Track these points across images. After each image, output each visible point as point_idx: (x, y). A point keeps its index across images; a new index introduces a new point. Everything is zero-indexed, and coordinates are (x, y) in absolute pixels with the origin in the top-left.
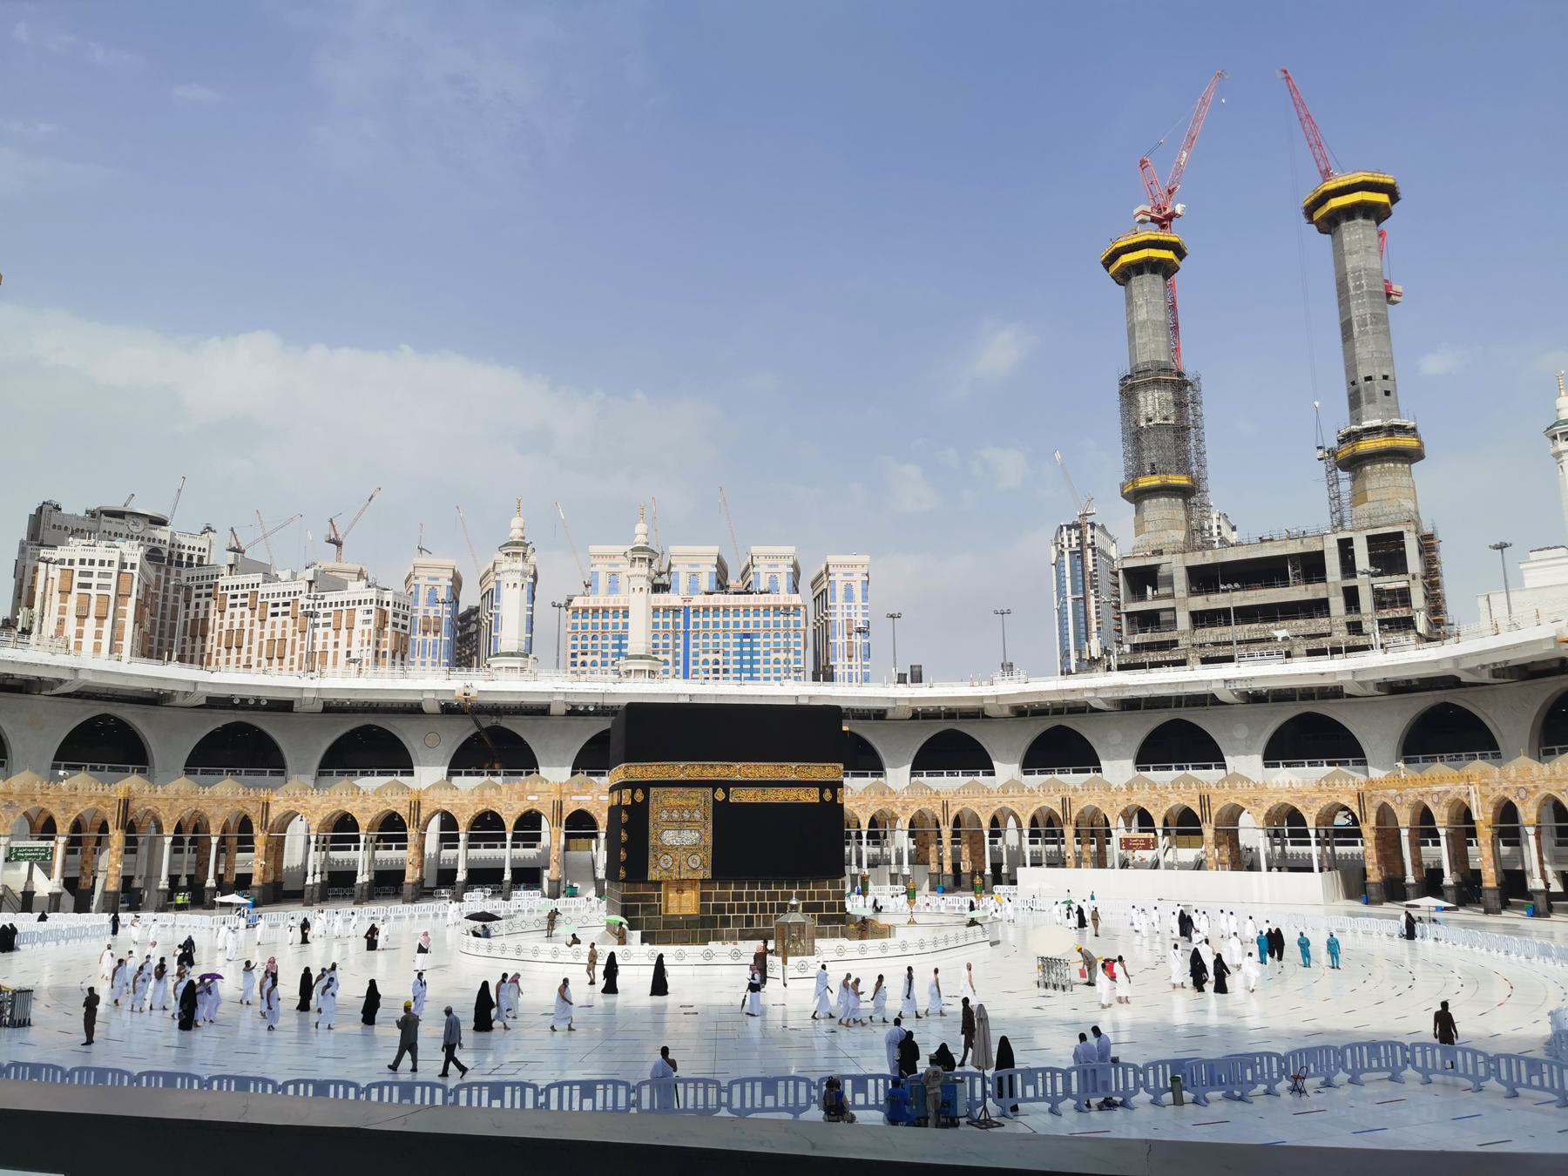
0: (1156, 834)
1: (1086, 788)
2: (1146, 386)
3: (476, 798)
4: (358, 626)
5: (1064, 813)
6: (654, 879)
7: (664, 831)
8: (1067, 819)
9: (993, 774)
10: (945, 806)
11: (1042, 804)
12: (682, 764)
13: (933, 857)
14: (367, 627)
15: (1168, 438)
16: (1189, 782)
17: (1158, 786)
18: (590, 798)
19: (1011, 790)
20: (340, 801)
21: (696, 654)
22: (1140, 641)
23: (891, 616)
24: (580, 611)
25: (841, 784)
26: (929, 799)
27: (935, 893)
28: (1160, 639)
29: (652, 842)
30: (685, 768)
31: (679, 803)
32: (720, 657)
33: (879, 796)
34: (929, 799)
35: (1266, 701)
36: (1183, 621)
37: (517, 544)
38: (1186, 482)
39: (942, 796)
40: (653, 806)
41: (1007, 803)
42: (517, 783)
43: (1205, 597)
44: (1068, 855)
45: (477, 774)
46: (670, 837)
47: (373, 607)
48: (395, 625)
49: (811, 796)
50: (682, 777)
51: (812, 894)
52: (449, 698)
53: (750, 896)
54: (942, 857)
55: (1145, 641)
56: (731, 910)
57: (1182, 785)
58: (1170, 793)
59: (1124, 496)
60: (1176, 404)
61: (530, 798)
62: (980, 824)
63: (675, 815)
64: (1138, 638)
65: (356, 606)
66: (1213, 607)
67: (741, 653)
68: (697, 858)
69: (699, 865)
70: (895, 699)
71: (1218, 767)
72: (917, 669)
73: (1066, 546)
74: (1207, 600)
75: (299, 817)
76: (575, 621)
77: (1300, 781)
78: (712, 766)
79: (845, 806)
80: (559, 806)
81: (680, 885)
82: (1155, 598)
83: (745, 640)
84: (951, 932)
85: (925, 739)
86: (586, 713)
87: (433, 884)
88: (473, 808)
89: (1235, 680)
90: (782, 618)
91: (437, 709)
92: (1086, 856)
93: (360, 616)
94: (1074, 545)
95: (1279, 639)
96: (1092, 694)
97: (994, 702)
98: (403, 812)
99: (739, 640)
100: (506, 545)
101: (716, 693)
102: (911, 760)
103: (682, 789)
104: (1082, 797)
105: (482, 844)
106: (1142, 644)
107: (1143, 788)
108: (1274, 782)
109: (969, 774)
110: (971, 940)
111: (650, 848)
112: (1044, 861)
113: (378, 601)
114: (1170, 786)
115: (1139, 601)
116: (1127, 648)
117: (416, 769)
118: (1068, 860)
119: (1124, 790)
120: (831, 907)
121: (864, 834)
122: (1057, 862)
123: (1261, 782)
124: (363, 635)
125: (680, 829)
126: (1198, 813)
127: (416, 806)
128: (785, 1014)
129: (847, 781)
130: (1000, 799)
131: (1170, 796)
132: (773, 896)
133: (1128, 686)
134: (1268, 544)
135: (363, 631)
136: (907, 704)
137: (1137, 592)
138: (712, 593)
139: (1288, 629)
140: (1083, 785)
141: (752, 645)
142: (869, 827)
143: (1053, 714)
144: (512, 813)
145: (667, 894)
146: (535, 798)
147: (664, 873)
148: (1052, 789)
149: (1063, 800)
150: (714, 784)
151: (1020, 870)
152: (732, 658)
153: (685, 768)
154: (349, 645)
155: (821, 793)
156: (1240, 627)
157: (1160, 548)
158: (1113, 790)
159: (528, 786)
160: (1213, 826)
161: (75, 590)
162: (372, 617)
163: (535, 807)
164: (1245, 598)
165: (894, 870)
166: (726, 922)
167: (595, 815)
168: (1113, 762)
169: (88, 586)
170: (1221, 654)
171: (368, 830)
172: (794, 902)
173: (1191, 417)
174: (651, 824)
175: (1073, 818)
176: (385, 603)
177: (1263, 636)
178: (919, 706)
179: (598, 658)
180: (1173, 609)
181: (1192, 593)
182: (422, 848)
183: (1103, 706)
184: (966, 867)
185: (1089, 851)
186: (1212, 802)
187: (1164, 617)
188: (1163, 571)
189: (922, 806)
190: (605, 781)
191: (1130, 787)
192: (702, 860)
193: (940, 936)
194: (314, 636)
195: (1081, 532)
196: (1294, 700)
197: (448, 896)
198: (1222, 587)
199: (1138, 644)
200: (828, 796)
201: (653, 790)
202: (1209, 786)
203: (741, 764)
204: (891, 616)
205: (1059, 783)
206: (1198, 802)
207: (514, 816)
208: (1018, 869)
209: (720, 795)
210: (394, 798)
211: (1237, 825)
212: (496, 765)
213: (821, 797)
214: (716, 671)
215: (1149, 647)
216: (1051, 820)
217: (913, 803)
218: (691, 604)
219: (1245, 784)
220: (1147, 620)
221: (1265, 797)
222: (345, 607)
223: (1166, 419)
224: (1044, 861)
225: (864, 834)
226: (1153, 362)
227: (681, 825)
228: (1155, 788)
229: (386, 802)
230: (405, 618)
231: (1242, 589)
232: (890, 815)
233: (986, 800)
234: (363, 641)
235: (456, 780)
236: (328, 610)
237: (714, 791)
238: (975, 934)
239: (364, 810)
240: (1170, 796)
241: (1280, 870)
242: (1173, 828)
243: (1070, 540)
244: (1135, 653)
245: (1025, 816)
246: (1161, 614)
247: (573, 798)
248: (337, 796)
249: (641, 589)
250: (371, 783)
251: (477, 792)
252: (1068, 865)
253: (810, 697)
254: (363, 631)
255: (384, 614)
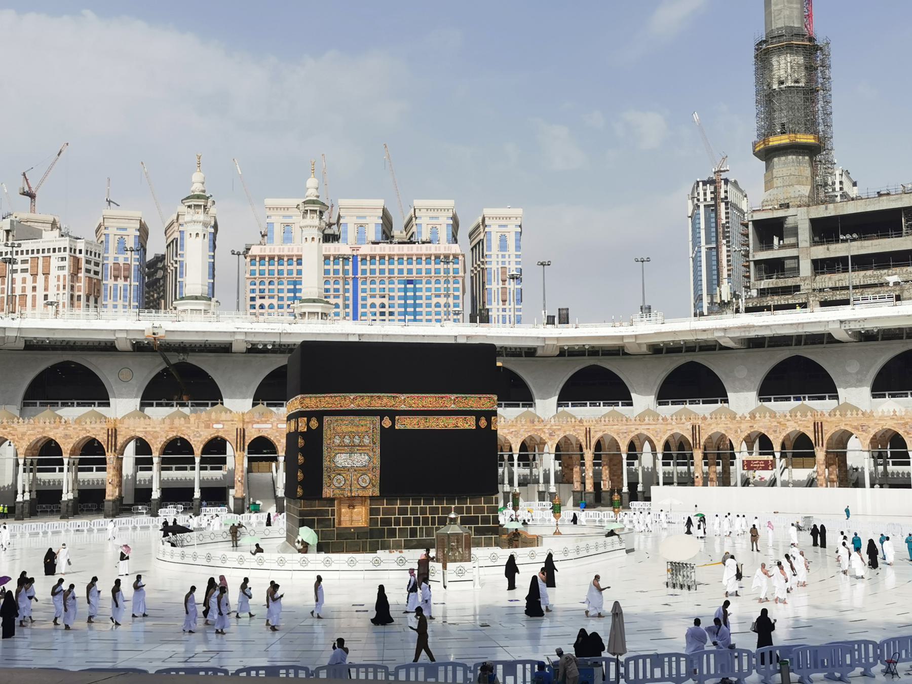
0: (774, 457)
1: (714, 416)
2: (780, 50)
3: (166, 426)
4: (54, 272)
5: (693, 435)
6: (328, 496)
7: (337, 454)
8: (696, 444)
9: (631, 404)
10: (588, 432)
11: (675, 431)
12: (352, 396)
13: (576, 477)
14: (61, 273)
15: (798, 100)
16: (805, 411)
17: (778, 415)
18: (270, 426)
19: (647, 419)
20: (44, 428)
21: (364, 299)
22: (766, 286)
23: (542, 264)
24: (258, 259)
25: (494, 413)
26: (574, 427)
27: (578, 508)
28: (784, 285)
29: (326, 464)
30: (355, 399)
31: (350, 429)
32: (386, 301)
33: (528, 424)
34: (574, 427)
35: (877, 340)
36: (806, 268)
37: (198, 197)
38: (813, 141)
39: (585, 424)
40: (327, 433)
41: (643, 430)
42: (204, 413)
43: (826, 246)
44: (696, 475)
45: (167, 405)
46: (342, 460)
47: (66, 254)
48: (88, 271)
49: (468, 423)
50: (353, 407)
51: (469, 509)
52: (139, 337)
53: (414, 511)
54: (584, 477)
55: (771, 286)
56: (397, 522)
57: (799, 414)
58: (788, 420)
59: (756, 154)
60: (806, 68)
61: (215, 426)
62: (618, 449)
63: (347, 441)
64: (765, 284)
65: (51, 254)
66: (833, 255)
67: (405, 298)
68: (367, 478)
69: (369, 484)
70: (545, 339)
71: (831, 398)
72: (565, 312)
73: (702, 200)
74: (828, 249)
75: (7, 443)
76: (253, 268)
77: (903, 410)
78: (379, 397)
79: (500, 433)
80: (242, 434)
81: (352, 502)
82: (781, 247)
83: (409, 286)
84: (591, 542)
85: (570, 374)
86: (265, 351)
87: (132, 502)
88: (165, 435)
89: (850, 321)
90: (442, 266)
91: (129, 348)
92: (712, 476)
93: (54, 263)
94: (709, 199)
95: (891, 284)
96: (721, 334)
97: (634, 340)
98: (102, 438)
99: (403, 286)
100: (188, 198)
101: (383, 333)
102: (558, 393)
103: (352, 417)
104: (710, 425)
105: (174, 466)
106: (768, 289)
107: (765, 417)
108: (880, 410)
109: (610, 405)
110: (609, 548)
111: (325, 469)
112: (675, 480)
113: (71, 249)
114: (788, 415)
115: (766, 250)
116: (754, 293)
117: (112, 401)
118: (696, 480)
119: (748, 418)
120: (486, 520)
121: (516, 457)
122: (687, 481)
123: (868, 411)
124: (58, 280)
125: (351, 453)
126: (812, 438)
127: (113, 433)
128: (445, 612)
129: (500, 411)
130: (637, 427)
131: (788, 423)
132: (434, 511)
133: (754, 326)
134: (884, 198)
135: (59, 277)
136: (555, 343)
137: (765, 241)
138: (378, 243)
139: (899, 275)
140: (711, 414)
141: (415, 290)
142: (520, 451)
143: (686, 351)
144: (199, 439)
145: (340, 510)
146: (220, 426)
147: (337, 491)
148: (683, 417)
149: (694, 428)
150: (381, 414)
151: (654, 489)
152: (397, 302)
153: (355, 399)
154: (46, 289)
155: (477, 421)
156: (856, 273)
157: (787, 201)
158: (738, 419)
159: (213, 416)
160: (825, 449)
162: (66, 263)
163: (220, 434)
164: (862, 247)
165: (542, 488)
166: (392, 533)
167: (275, 441)
168: (739, 394)
170: (838, 298)
171: (71, 454)
172: (452, 516)
173: (820, 80)
174: (325, 448)
175: (702, 443)
176: (77, 252)
177: (876, 282)
178: (566, 344)
179: (275, 302)
180: (797, 258)
181: (814, 243)
182: (119, 469)
183: (731, 344)
184: (606, 485)
185: (715, 472)
186: (825, 428)
187: (789, 264)
188: (790, 223)
189: (568, 433)
190: (283, 411)
191: (753, 416)
192: (371, 480)
193: (582, 545)
194: (13, 281)
195: (715, 188)
196: (902, 338)
197: (145, 511)
198: (842, 237)
199: (764, 289)
200: (483, 423)
201: (326, 419)
202: (822, 414)
203: (405, 395)
204: (542, 264)
205: (691, 412)
206: (812, 428)
207: (201, 442)
208: (652, 487)
209: (387, 423)
210: (93, 426)
211: (846, 448)
212: (185, 397)
213: (477, 424)
214: (382, 314)
215: (774, 291)
216: (683, 444)
217: (559, 429)
218: (359, 253)
219: (855, 412)
220: (774, 267)
221: (872, 424)
222: (41, 255)
223: (797, 81)
224: (675, 480)
225: (516, 457)
226: (786, 27)
227: (352, 449)
228: (775, 416)
229: (86, 430)
230: (97, 264)
231: (860, 239)
232: (538, 440)
233: (625, 427)
234: (58, 286)
235: (148, 410)
237: (382, 419)
238: (613, 544)
239: (66, 436)
240: (788, 423)
241: (881, 486)
242: (789, 451)
243: (705, 194)
244: (761, 297)
245: (659, 441)
246: (787, 262)
247: (255, 426)
248: (41, 424)
249: (313, 239)
250: (72, 413)
251: (167, 421)
252: (696, 484)
253: (468, 337)
254: (59, 277)
255: (77, 261)
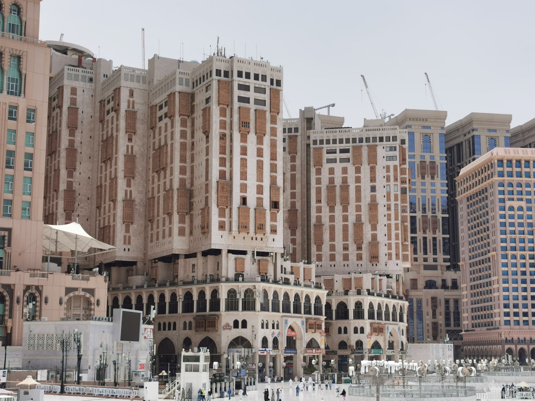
4: (381, 162)
14: (391, 164)
65: (378, 143)
93: (381, 152)
124: (388, 170)
161: (236, 104)
169: (246, 100)
194: (332, 171)
222: (364, 143)
236: (344, 146)
